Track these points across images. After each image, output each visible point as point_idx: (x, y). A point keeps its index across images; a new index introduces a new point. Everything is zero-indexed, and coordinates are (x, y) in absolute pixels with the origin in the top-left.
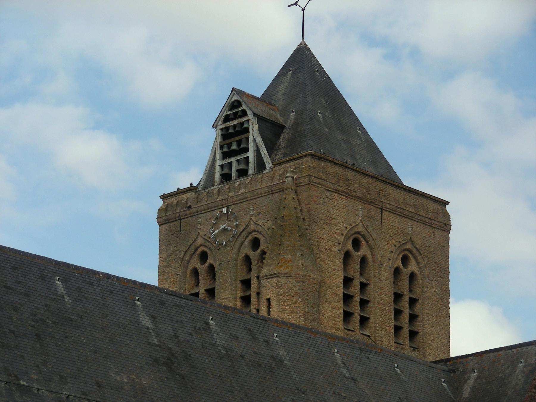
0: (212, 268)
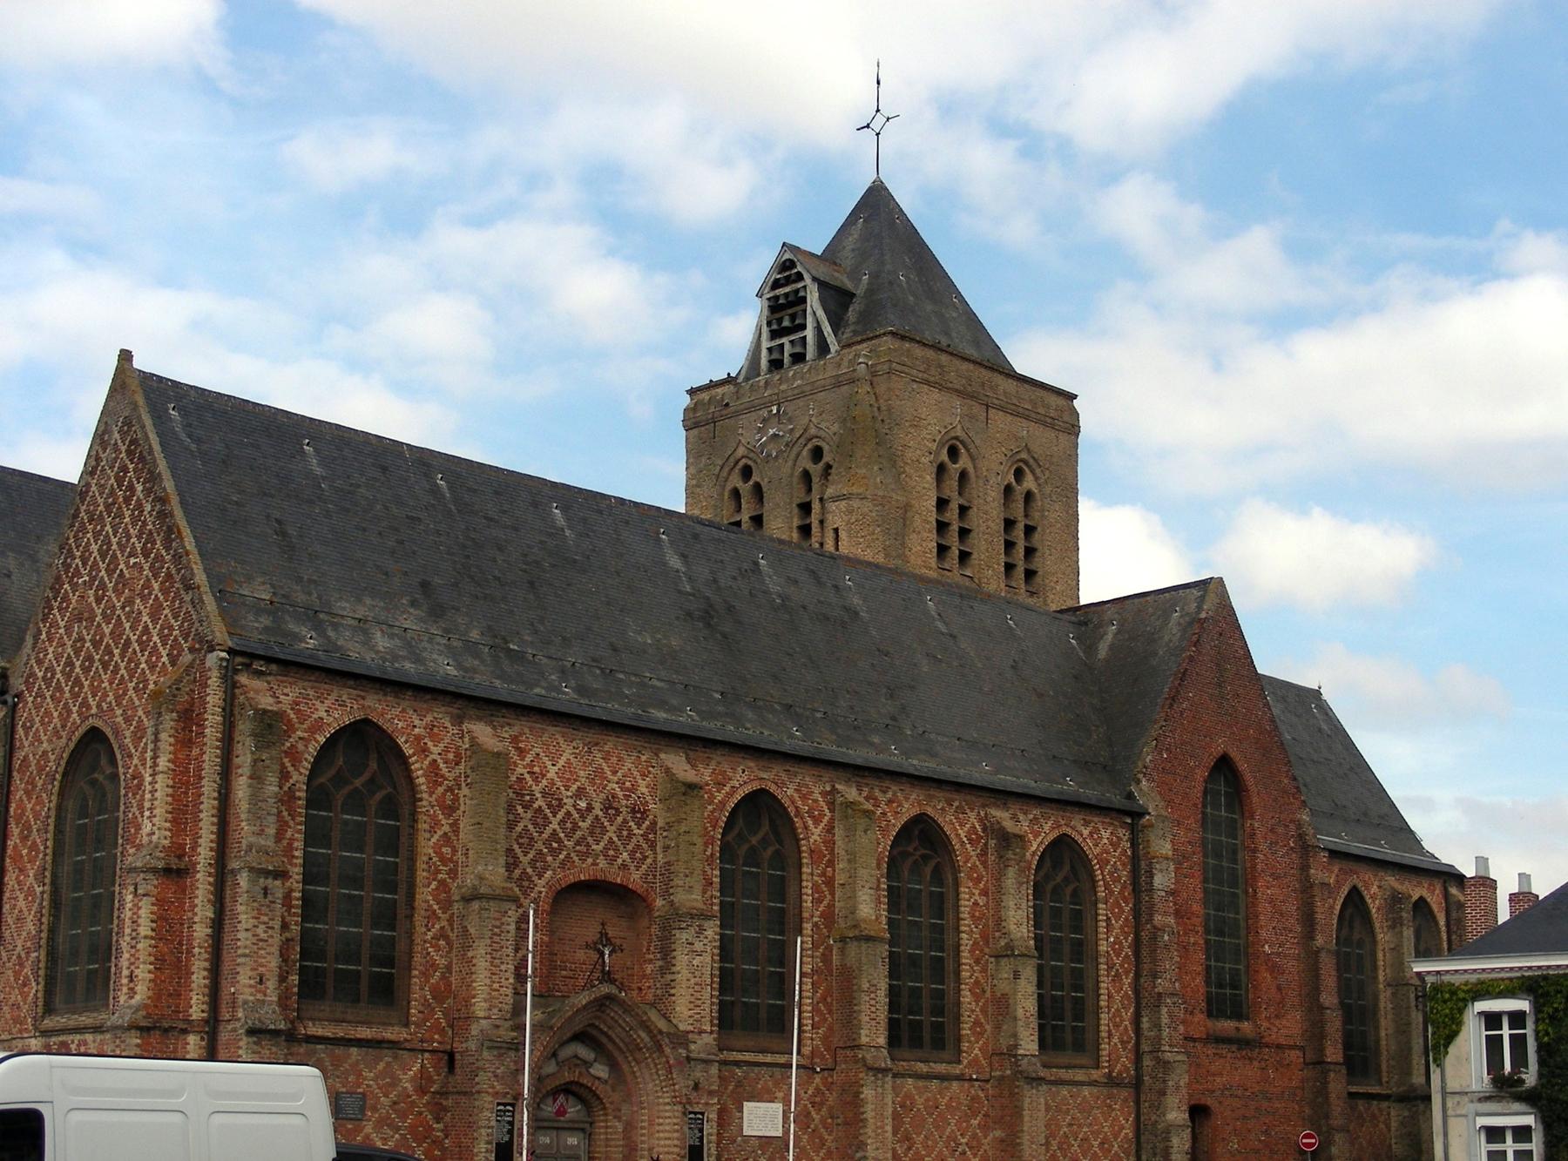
0: (758, 488)
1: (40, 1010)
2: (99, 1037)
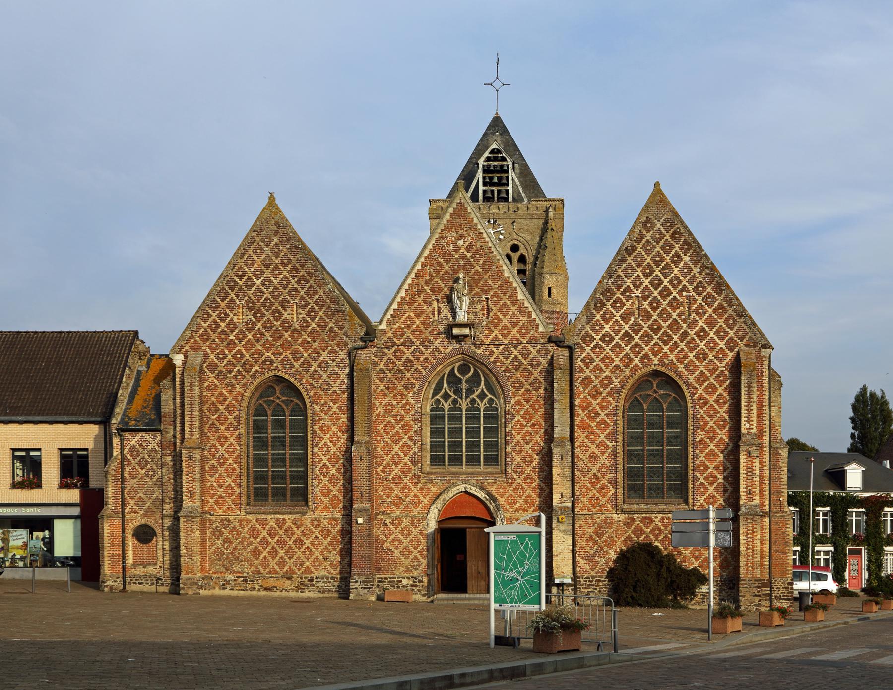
1: (620, 501)
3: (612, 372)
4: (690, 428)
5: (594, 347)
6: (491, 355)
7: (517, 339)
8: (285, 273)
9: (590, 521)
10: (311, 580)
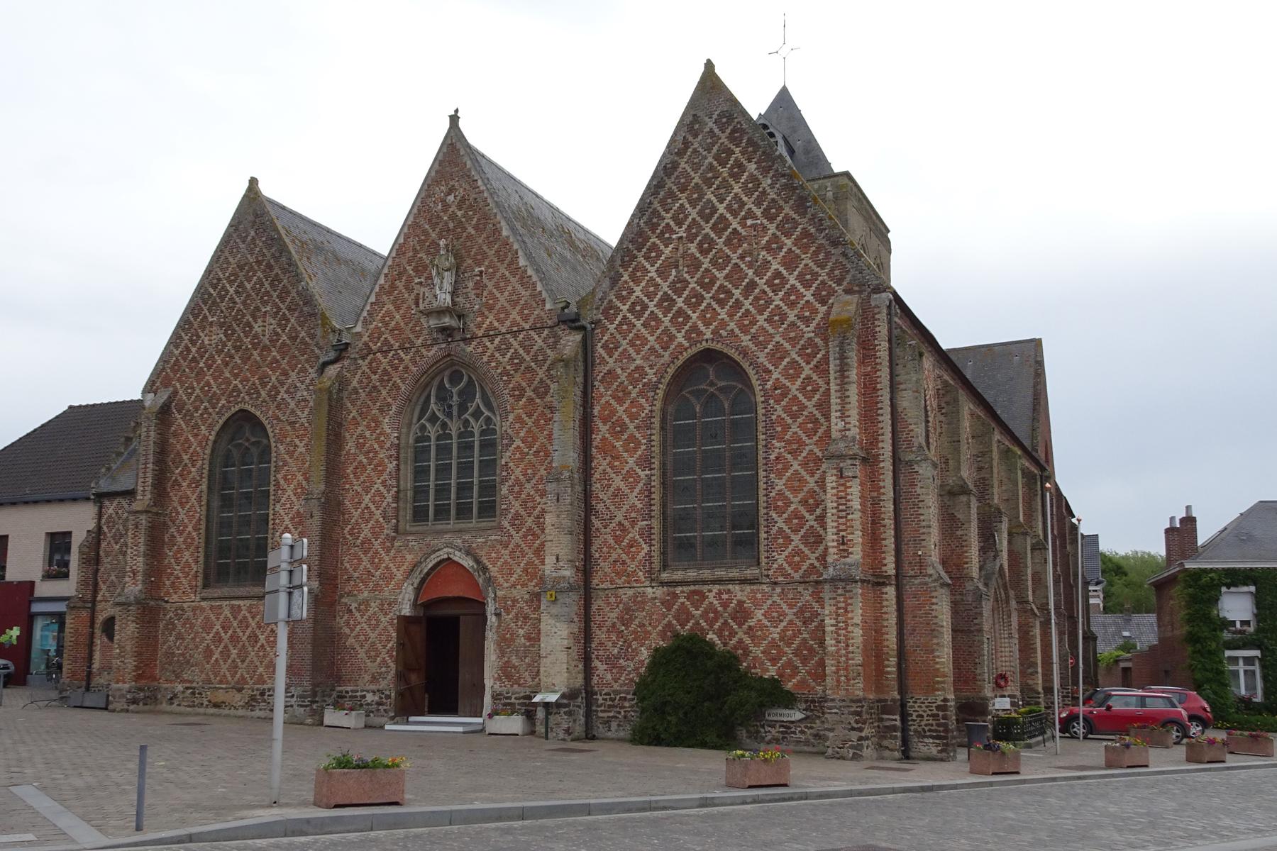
1: (656, 565)
2: (748, 588)
3: (645, 359)
4: (762, 437)
5: (621, 324)
6: (484, 353)
7: (518, 325)
8: (259, 274)
9: (612, 600)
10: (262, 694)
